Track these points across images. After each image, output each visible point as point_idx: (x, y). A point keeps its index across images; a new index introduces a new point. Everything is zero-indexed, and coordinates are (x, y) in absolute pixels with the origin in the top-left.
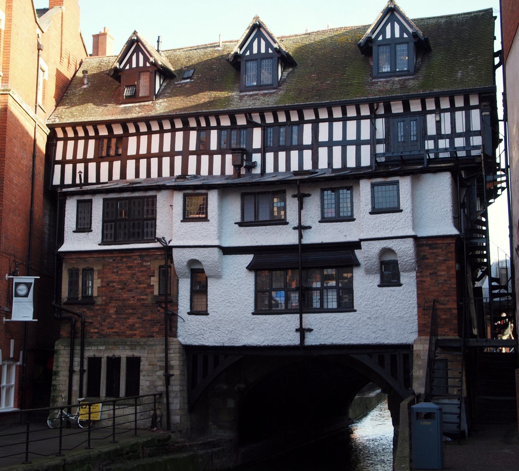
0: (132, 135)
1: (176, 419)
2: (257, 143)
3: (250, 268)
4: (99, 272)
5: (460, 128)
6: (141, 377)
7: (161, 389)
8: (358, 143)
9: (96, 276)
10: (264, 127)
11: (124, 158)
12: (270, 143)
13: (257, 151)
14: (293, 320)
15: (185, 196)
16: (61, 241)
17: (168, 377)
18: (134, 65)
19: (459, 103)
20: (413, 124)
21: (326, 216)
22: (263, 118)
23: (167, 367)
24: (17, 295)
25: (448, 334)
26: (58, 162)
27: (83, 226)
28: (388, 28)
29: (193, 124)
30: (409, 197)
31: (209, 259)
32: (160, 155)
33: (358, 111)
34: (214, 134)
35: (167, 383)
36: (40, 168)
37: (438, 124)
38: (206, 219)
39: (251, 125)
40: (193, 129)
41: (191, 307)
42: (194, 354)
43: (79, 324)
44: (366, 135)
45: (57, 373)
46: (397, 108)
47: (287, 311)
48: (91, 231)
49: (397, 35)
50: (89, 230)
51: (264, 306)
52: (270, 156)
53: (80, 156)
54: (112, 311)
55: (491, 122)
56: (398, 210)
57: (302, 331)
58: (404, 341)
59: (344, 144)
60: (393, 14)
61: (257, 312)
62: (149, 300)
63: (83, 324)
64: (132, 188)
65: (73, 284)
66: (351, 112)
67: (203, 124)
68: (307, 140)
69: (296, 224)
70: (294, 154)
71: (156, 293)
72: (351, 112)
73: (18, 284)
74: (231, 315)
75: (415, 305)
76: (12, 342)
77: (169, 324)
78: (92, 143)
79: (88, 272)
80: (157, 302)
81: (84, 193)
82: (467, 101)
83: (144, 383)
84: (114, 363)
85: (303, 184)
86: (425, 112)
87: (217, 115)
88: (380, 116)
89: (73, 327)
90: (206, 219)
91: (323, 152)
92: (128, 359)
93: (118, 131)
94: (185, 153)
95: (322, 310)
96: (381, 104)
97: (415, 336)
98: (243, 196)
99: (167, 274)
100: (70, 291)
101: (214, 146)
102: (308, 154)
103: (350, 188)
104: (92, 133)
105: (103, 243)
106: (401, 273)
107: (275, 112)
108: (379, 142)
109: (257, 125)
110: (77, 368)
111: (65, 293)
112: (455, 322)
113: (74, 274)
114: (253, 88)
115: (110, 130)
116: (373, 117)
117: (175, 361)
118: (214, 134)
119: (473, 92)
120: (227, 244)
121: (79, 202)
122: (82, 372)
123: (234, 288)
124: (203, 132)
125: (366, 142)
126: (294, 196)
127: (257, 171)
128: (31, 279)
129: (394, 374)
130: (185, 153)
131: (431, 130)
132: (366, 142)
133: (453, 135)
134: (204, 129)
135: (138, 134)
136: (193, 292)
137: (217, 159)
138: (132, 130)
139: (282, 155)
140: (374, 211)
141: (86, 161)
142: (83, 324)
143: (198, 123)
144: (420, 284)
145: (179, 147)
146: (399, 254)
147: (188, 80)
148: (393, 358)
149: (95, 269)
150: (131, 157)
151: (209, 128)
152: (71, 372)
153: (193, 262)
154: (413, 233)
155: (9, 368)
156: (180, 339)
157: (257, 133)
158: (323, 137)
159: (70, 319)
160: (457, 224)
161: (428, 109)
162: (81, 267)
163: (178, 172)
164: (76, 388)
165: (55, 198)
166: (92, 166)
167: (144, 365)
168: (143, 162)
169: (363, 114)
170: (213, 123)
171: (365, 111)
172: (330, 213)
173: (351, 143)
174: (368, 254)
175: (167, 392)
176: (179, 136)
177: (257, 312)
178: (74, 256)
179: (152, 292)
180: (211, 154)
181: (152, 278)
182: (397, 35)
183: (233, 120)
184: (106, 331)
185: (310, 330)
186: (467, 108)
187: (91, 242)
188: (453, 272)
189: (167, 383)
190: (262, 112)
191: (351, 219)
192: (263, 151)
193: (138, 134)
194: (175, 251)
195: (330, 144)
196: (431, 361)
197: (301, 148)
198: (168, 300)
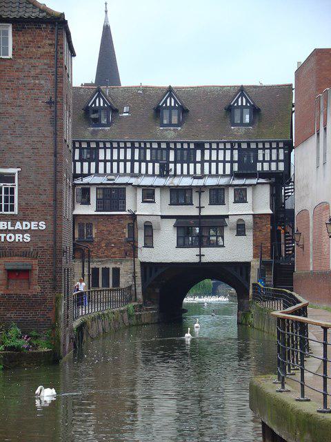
0: (101, 148)
2: (172, 158)
5: (274, 158)
8: (224, 162)
9: (94, 228)
10: (175, 149)
11: (97, 161)
12: (179, 158)
13: (172, 162)
14: (196, 251)
15: (143, 190)
17: (134, 277)
18: (97, 105)
19: (274, 145)
20: (252, 154)
22: (175, 145)
23: (134, 273)
25: (267, 258)
29: (137, 145)
32: (118, 161)
34: (148, 152)
37: (264, 155)
38: (154, 202)
39: (168, 149)
41: (145, 244)
44: (228, 158)
52: (179, 166)
56: (246, 202)
57: (200, 256)
58: (247, 260)
59: (217, 162)
61: (178, 246)
63: (89, 251)
65: (81, 231)
66: (221, 146)
67: (143, 145)
68: (198, 158)
70: (192, 166)
71: (127, 236)
72: (221, 146)
74: (166, 249)
79: (90, 226)
82: (278, 145)
84: (106, 270)
86: (257, 149)
88: (235, 149)
90: (154, 202)
91: (206, 165)
94: (133, 161)
99: (133, 229)
100: (80, 235)
101: (148, 158)
102: (198, 166)
109: (172, 149)
110: (86, 273)
113: (81, 225)
116: (232, 149)
117: (138, 270)
118: (148, 152)
119: (281, 141)
122: (89, 275)
124: (143, 150)
125: (228, 162)
127: (172, 173)
131: (260, 158)
133: (271, 161)
135: (105, 148)
137: (150, 165)
138: (101, 145)
139: (185, 165)
140: (235, 202)
143: (140, 145)
145: (129, 157)
147: (127, 114)
148: (241, 269)
150: (101, 161)
151: (145, 148)
157: (172, 154)
158: (207, 157)
162: (85, 222)
168: (108, 164)
170: (148, 146)
171: (228, 146)
174: (232, 221)
175: (135, 284)
176: (129, 151)
177: (178, 246)
180: (147, 162)
186: (278, 148)
187: (90, 210)
188: (269, 230)
192: (175, 163)
193: (105, 148)
197: (195, 163)
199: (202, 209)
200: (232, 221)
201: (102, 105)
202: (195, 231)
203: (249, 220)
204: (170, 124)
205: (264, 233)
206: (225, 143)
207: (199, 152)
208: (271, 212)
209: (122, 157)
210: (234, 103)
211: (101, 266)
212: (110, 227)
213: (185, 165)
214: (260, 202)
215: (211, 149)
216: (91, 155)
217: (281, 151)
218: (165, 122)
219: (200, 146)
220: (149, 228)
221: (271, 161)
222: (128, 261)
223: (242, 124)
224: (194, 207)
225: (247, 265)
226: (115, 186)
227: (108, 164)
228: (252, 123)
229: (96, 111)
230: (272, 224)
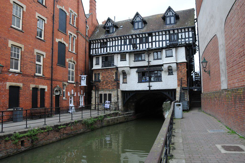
0: (109, 42)
1: (120, 108)
3: (137, 72)
4: (101, 74)
5: (187, 36)
6: (112, 98)
7: (117, 101)
10: (139, 38)
11: (107, 47)
15: (121, 55)
16: (92, 67)
18: (109, 25)
19: (187, 30)
20: (175, 36)
21: (155, 58)
22: (139, 36)
23: (118, 96)
24: (82, 80)
25: (185, 86)
26: (92, 49)
27: (97, 64)
28: (169, 13)
29: (123, 38)
30: (175, 53)
31: (126, 70)
32: (115, 46)
33: (162, 33)
34: (128, 40)
35: (118, 99)
36: (87, 50)
37: (182, 35)
38: (126, 60)
39: (137, 38)
40: (123, 39)
42: (123, 92)
43: (97, 86)
44: (164, 39)
45: (92, 98)
46: (172, 32)
47: (146, 82)
48: (99, 64)
49: (171, 15)
50: (99, 64)
51: (140, 81)
52: (141, 45)
53: (97, 47)
54: (105, 83)
55: (194, 35)
56: (172, 56)
58: (174, 88)
60: (170, 10)
62: (113, 80)
63: (98, 86)
64: (108, 54)
65: (95, 77)
66: (160, 33)
67: (125, 38)
68: (150, 41)
69: (148, 61)
71: (115, 78)
72: (160, 33)
73: (82, 77)
74: (133, 83)
75: (177, 79)
76: (82, 91)
77: (118, 86)
78: (99, 44)
79: (99, 74)
80: (115, 81)
81: (97, 56)
82: (188, 30)
83: (113, 100)
84: (105, 95)
85: (149, 51)
86: (178, 33)
87: (128, 36)
88: (167, 34)
89: (96, 87)
90: (126, 60)
91: (154, 43)
92: (109, 94)
93: (105, 41)
94: (121, 45)
95: (154, 81)
96: (168, 32)
97: (177, 87)
98: (135, 54)
99: (116, 73)
101: (128, 43)
102: (150, 44)
103: (160, 52)
104: (99, 42)
105: (102, 67)
106: (173, 72)
107: (142, 34)
108: (167, 40)
109: (138, 38)
110: (97, 97)
111: (94, 79)
112: (186, 83)
113: (95, 74)
114: (137, 29)
115: (103, 41)
116: (166, 34)
117: (120, 94)
118: (128, 40)
119: (190, 27)
120: (131, 66)
121: (96, 58)
123: (133, 76)
125: (164, 41)
126: (147, 54)
127: (138, 48)
128: (85, 76)
129: (172, 96)
130: (121, 45)
131: (180, 37)
132: (164, 41)
133: (185, 38)
134: (125, 39)
135: (110, 41)
136: (123, 78)
137: (129, 46)
138: (108, 40)
140: (166, 57)
141: (98, 48)
142: (98, 86)
144: (178, 74)
145: (120, 44)
146: (173, 67)
149: (100, 73)
151: (126, 39)
152: (96, 97)
153: (123, 71)
154: (176, 62)
155: (82, 97)
156: (121, 89)
157: (138, 40)
158: (154, 40)
159: (95, 85)
160: (186, 59)
161: (179, 32)
163: (119, 50)
164: (97, 101)
165: (91, 57)
166: (99, 49)
167: (112, 96)
168: (111, 48)
169: (163, 34)
170: (127, 38)
171: (164, 33)
172: (156, 58)
173: (161, 41)
174: (165, 67)
176: (120, 41)
178: (95, 70)
179: (114, 78)
181: (114, 75)
182: (171, 15)
183: (132, 37)
184: (103, 88)
185: (152, 86)
186: (188, 31)
187: (99, 67)
189: (118, 99)
190: (139, 34)
191: (161, 59)
192: (139, 44)
193: (110, 41)
194: (119, 68)
195: (156, 41)
196: (181, 93)
197: (149, 43)
198: (117, 80)
199: (150, 63)
200: (165, 67)
201: (110, 25)
202: (146, 73)
203: (174, 66)
204: (138, 29)
205: (183, 73)
206: (162, 32)
207: (150, 38)
208: (185, 61)
209: (117, 44)
210: (166, 15)
211: (102, 92)
212: (107, 74)
213: (144, 45)
214: (181, 55)
215: (156, 36)
216: (104, 45)
217: (191, 33)
218: (136, 27)
219: (150, 34)
220: (124, 74)
221: (185, 38)
222: (115, 90)
223: (170, 24)
224: (146, 62)
225: (174, 91)
226: (109, 55)
227: (111, 48)
228: (175, 23)
229: (108, 28)
230: (187, 68)
